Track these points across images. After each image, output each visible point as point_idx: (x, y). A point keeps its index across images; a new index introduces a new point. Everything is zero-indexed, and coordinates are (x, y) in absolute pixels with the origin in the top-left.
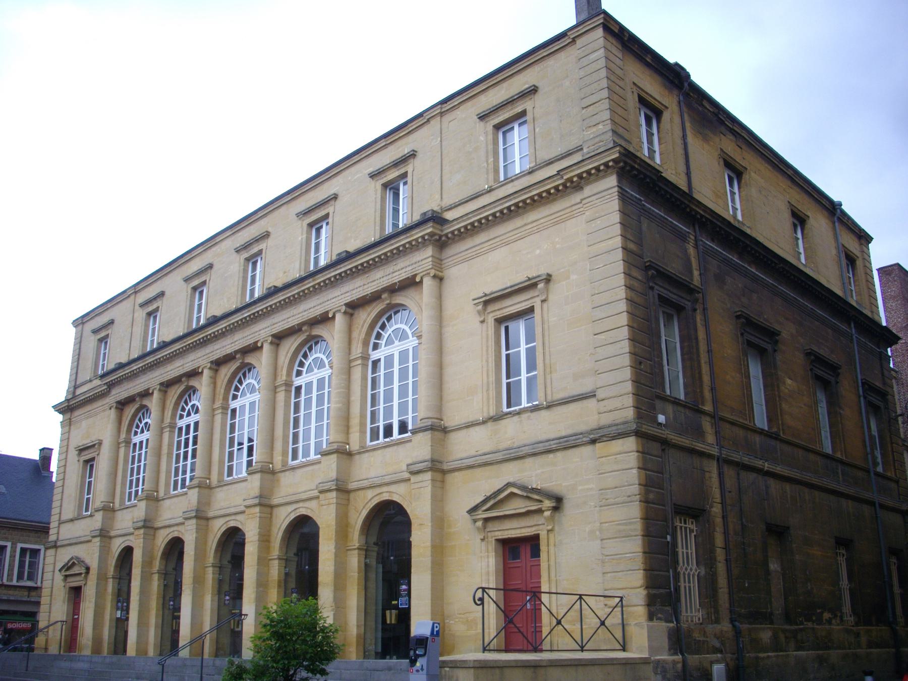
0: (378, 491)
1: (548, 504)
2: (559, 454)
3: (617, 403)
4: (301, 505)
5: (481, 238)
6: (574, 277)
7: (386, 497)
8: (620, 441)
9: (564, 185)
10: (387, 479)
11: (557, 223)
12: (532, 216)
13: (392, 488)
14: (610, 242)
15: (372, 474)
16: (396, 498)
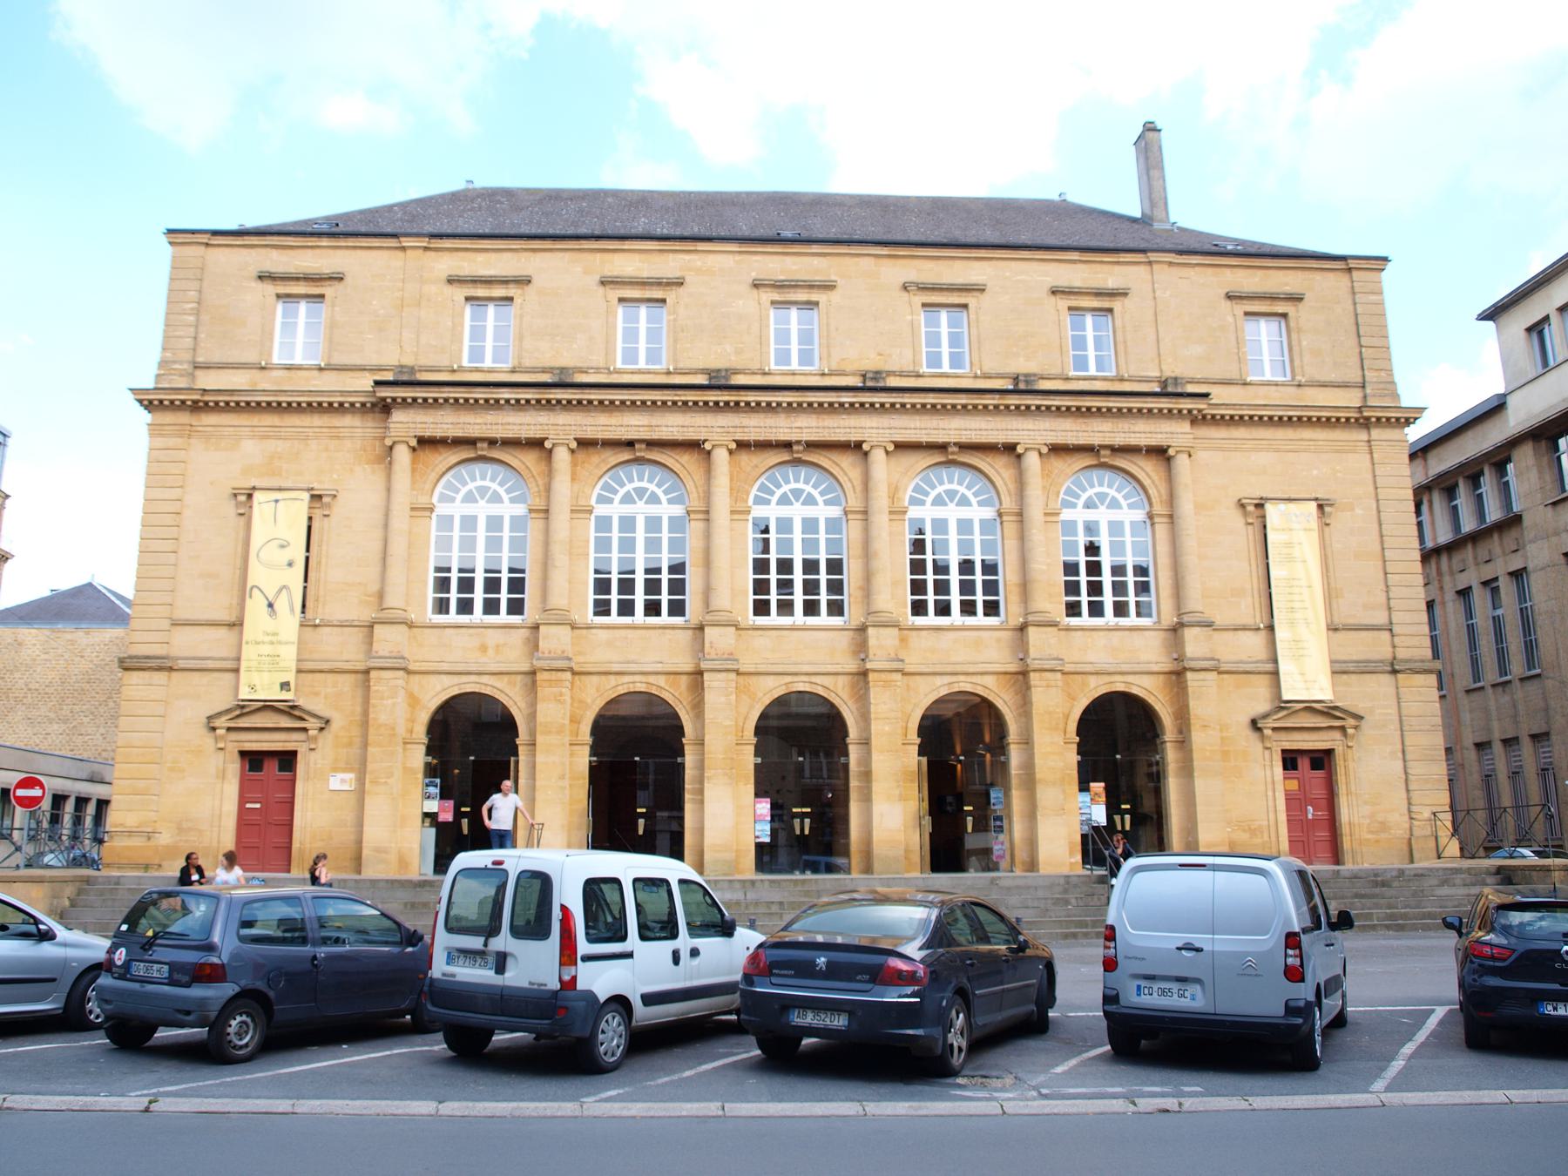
0: (1107, 679)
1: (1351, 722)
2: (1353, 677)
3: (1415, 641)
4: (962, 678)
5: (1241, 432)
6: (1358, 511)
7: (1120, 687)
8: (1422, 677)
9: (1357, 419)
10: (1125, 668)
11: (1337, 451)
12: (1307, 433)
13: (1130, 678)
14: (1402, 492)
15: (1091, 657)
16: (1135, 691)
